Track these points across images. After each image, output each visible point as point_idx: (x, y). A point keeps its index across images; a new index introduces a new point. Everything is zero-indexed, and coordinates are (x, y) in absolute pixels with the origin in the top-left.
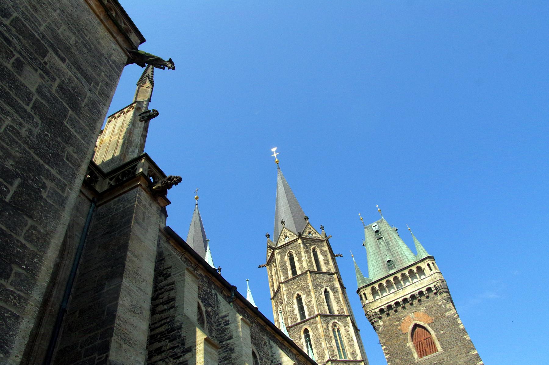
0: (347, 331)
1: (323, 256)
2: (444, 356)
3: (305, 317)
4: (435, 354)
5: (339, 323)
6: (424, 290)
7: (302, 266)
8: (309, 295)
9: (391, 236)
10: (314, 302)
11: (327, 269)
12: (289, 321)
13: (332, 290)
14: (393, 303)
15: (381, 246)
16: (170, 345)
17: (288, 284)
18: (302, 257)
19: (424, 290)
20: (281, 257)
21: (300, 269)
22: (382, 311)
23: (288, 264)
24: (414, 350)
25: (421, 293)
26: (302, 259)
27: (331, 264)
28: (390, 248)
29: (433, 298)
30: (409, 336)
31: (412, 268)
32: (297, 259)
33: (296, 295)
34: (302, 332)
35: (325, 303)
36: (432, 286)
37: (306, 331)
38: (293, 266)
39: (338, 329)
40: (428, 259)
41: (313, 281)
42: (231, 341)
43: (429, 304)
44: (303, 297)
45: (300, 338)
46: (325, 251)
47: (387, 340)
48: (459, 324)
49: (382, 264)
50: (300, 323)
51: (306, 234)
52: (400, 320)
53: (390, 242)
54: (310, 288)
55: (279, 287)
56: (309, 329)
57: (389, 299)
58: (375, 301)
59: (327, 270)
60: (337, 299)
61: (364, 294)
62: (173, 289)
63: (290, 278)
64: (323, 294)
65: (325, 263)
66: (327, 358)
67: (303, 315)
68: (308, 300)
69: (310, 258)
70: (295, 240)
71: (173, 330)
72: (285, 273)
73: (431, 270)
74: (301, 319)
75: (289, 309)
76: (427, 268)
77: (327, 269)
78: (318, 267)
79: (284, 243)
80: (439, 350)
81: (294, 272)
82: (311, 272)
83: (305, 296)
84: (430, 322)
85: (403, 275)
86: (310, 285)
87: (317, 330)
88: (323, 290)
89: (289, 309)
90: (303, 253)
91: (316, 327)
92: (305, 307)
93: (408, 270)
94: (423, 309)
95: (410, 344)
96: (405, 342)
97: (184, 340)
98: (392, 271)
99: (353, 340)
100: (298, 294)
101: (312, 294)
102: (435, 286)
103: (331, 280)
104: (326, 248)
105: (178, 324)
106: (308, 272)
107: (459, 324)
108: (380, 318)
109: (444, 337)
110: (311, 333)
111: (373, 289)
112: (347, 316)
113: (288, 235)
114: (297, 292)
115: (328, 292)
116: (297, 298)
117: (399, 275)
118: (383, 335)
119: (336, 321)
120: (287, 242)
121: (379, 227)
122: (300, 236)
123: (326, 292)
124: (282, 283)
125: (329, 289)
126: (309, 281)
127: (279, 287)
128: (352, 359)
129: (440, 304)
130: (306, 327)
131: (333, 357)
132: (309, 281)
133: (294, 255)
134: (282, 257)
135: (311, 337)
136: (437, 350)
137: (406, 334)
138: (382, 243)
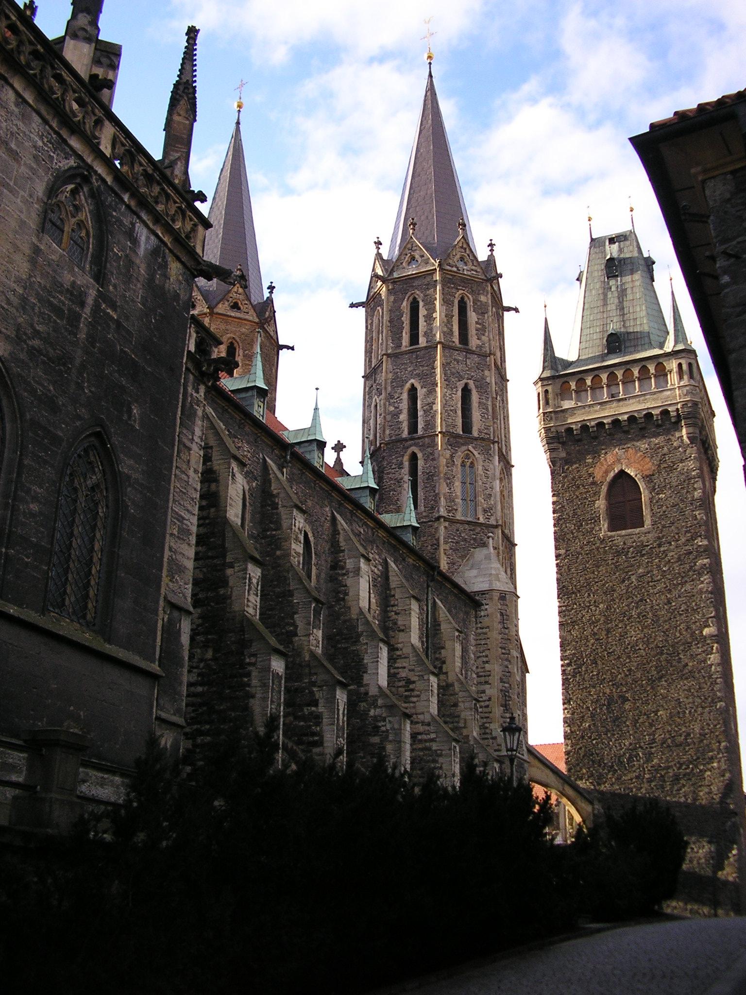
1: (477, 314)
4: (637, 530)
5: (476, 453)
8: (432, 391)
11: (478, 342)
12: (387, 432)
13: (476, 387)
15: (609, 295)
17: (399, 361)
20: (395, 301)
23: (406, 319)
25: (649, 416)
30: (604, 489)
32: (426, 313)
34: (406, 458)
35: (459, 413)
37: (414, 458)
40: (683, 355)
41: (443, 365)
44: (421, 392)
49: (599, 336)
50: (406, 440)
53: (629, 291)
56: (420, 455)
59: (480, 347)
63: (403, 349)
64: (459, 393)
67: (413, 428)
68: (430, 400)
69: (449, 316)
73: (681, 378)
74: (409, 434)
75: (392, 408)
78: (464, 337)
81: (414, 339)
82: (444, 347)
84: (647, 473)
86: (438, 371)
88: (460, 385)
89: (392, 408)
92: (420, 413)
95: (601, 504)
100: (413, 385)
101: (438, 389)
103: (479, 367)
108: (563, 443)
110: (420, 463)
113: (417, 256)
114: (412, 381)
115: (470, 391)
119: (470, 447)
123: (466, 392)
124: (388, 355)
125: (471, 384)
128: (482, 520)
131: (449, 512)
132: (438, 363)
133: (421, 304)
134: (398, 302)
135: (420, 468)
138: (613, 289)
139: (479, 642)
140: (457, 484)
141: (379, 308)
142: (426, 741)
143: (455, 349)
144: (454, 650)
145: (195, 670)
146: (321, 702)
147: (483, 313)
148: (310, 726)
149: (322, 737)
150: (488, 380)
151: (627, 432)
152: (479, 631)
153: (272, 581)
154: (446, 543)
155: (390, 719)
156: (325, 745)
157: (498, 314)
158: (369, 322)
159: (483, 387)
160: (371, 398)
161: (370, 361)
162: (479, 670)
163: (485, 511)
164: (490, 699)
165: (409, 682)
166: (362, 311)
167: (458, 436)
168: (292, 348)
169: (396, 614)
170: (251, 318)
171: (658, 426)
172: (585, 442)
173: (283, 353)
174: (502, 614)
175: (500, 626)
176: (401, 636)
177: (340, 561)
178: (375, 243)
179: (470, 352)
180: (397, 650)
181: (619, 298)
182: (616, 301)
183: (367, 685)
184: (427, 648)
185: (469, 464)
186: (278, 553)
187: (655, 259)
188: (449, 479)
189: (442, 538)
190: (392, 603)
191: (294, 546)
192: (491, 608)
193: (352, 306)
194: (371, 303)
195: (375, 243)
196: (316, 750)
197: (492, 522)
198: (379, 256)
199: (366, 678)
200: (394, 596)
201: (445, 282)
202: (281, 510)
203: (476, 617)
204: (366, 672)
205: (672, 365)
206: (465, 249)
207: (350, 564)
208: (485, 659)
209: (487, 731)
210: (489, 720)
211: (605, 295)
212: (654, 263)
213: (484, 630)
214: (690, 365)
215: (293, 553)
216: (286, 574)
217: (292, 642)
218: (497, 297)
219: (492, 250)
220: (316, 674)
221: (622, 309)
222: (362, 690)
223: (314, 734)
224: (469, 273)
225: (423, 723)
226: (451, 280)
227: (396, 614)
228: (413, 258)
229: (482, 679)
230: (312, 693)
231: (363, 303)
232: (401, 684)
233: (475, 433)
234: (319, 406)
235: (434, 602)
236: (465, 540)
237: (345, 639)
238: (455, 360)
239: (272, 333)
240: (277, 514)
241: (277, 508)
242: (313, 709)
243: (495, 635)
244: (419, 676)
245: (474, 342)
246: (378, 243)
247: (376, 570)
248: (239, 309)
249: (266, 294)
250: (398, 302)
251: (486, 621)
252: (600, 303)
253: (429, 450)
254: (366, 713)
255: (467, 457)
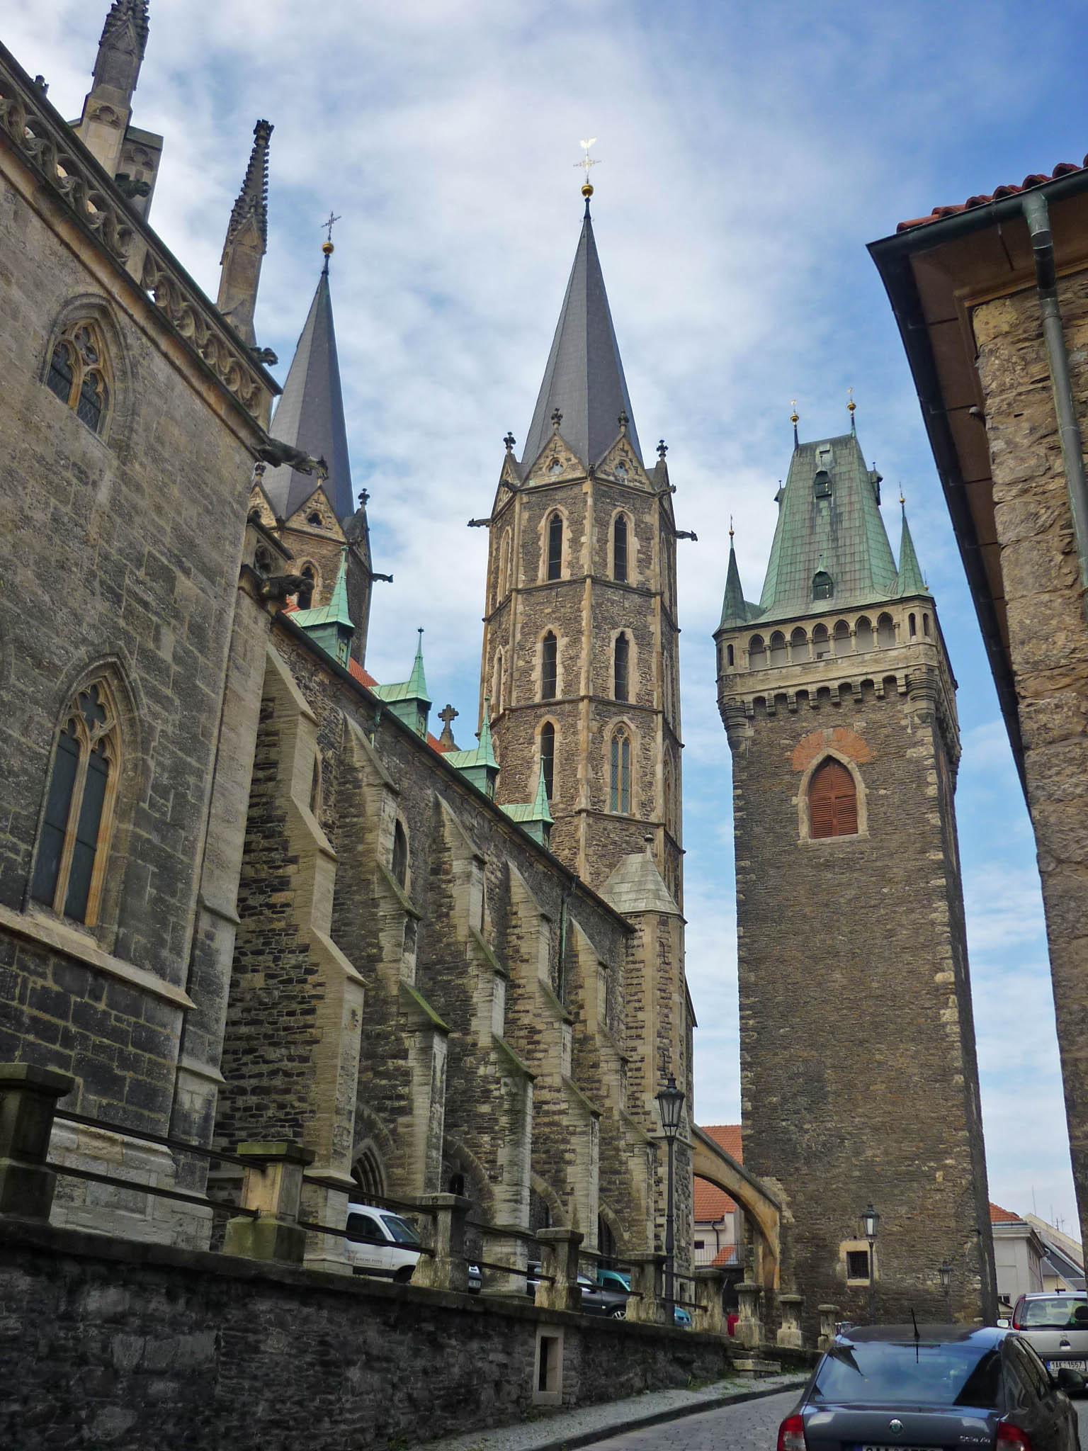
0: (646, 749)
1: (641, 539)
2: (865, 847)
3: (553, 695)
4: (847, 838)
5: (633, 726)
6: (878, 679)
7: (578, 558)
8: (575, 641)
9: (855, 498)
10: (583, 661)
11: (641, 578)
12: (514, 695)
13: (636, 637)
14: (792, 691)
15: (819, 521)
16: (264, 843)
17: (533, 600)
18: (582, 533)
19: (878, 679)
20: (530, 519)
21: (570, 565)
22: (759, 701)
23: (544, 543)
24: (804, 817)
25: (868, 684)
26: (583, 539)
27: (655, 566)
28: (840, 534)
29: (894, 703)
30: (805, 780)
31: (867, 613)
33: (543, 633)
34: (538, 730)
35: (612, 671)
36: (899, 675)
37: (548, 730)
38: (555, 552)
39: (626, 743)
40: (917, 603)
42: (361, 819)
43: (878, 716)
44: (561, 643)
45: (531, 743)
46: (649, 528)
47: (751, 777)
48: (929, 784)
49: (803, 575)
50: (539, 706)
51: (611, 467)
52: (796, 737)
53: (846, 516)
54: (584, 624)
55: (508, 599)
56: (557, 727)
57: (786, 678)
58: (751, 674)
59: (640, 583)
60: (643, 663)
61: (730, 647)
62: (274, 745)
63: (539, 583)
64: (613, 645)
65: (639, 561)
66: (583, 802)
67: (549, 688)
69: (602, 541)
70: (578, 482)
71: (269, 819)
72: (532, 568)
73: (913, 632)
74: (544, 697)
75: (521, 663)
76: (906, 625)
77: (641, 578)
79: (546, 480)
80: (860, 832)
81: (554, 570)
82: (595, 581)
83: (566, 639)
84: (862, 760)
85: (841, 626)
87: (575, 733)
88: (615, 634)
89: (521, 663)
90: (587, 523)
91: (574, 726)
92: (560, 670)
93: (857, 615)
94: (859, 724)
95: (800, 801)
96: (789, 793)
97: (287, 842)
98: (821, 606)
99: (653, 774)
100: (550, 632)
102: (906, 676)
104: (653, 519)
105: (279, 812)
106: (589, 581)
107: (929, 784)
108: (751, 718)
109: (883, 805)
110: (558, 738)
111: (757, 641)
112: (656, 713)
113: (562, 460)
114: (550, 626)
115: (627, 642)
116: (546, 639)
117: (830, 624)
118: (744, 763)
119: (625, 719)
120: (553, 479)
121: (835, 460)
122: (592, 473)
123: (622, 642)
124: (518, 591)
125: (629, 635)
126: (585, 604)
127: (508, 599)
128: (638, 817)
129: (903, 723)
130: (549, 718)
131: (594, 804)
132: (585, 604)
133: (565, 524)
135: (556, 745)
136: (855, 830)
137: (800, 773)
138: (825, 513)
139: (629, 981)
140: (607, 768)
141: (508, 528)
142: (554, 1113)
143: (607, 584)
144: (596, 990)
145: (239, 1004)
146: (412, 1054)
147: (649, 539)
148: (395, 1086)
149: (411, 1101)
150: (652, 628)
151: (837, 705)
152: (631, 966)
153: (350, 886)
154: (588, 845)
155: (507, 1080)
156: (416, 1112)
157: (668, 541)
158: (495, 546)
159: (644, 638)
160: (494, 649)
161: (494, 599)
162: (629, 1019)
163: (643, 805)
164: (642, 1060)
165: (533, 1031)
166: (485, 531)
167: (609, 703)
168: (390, 579)
169: (519, 938)
170: (335, 537)
171: (880, 698)
172: (781, 717)
173: (377, 586)
174: (662, 945)
175: (659, 961)
176: (524, 970)
177: (445, 863)
178: (505, 440)
179: (628, 589)
180: (519, 987)
181: (831, 524)
182: (828, 529)
183: (476, 1033)
184: (559, 986)
185: (621, 740)
186: (360, 848)
187: (881, 473)
188: (594, 759)
189: (582, 842)
190: (514, 923)
191: (381, 839)
192: (647, 935)
193: (472, 523)
194: (498, 521)
195: (505, 440)
196: (402, 1120)
197: (653, 818)
198: (510, 458)
199: (475, 1024)
200: (516, 913)
201: (599, 495)
202: (365, 789)
203: (627, 947)
204: (473, 1015)
205: (900, 616)
206: (627, 452)
207: (458, 866)
208: (637, 1005)
209: (638, 1103)
210: (640, 1088)
211: (812, 519)
212: (880, 479)
213: (637, 966)
214: (925, 616)
215: (380, 848)
216: (370, 877)
217: (374, 970)
218: (667, 518)
219: (663, 455)
220: (405, 1015)
221: (836, 540)
222: (469, 1039)
223: (400, 1097)
224: (631, 484)
225: (551, 1088)
226: (608, 491)
227: (519, 938)
228: (556, 462)
229: (633, 1032)
230: (399, 1040)
231: (488, 520)
232: (523, 1033)
233: (632, 700)
234: (423, 655)
235: (571, 924)
236: (615, 843)
237: (448, 969)
238: (608, 600)
239: (363, 558)
240: (360, 794)
241: (360, 787)
242: (401, 1062)
243: (649, 974)
244: (547, 1023)
245: (633, 578)
246: (510, 441)
247: (493, 878)
248: (319, 523)
249: (357, 505)
250: (534, 520)
251: (640, 954)
252: (806, 531)
253: (570, 719)
254: (472, 1072)
255: (620, 731)
